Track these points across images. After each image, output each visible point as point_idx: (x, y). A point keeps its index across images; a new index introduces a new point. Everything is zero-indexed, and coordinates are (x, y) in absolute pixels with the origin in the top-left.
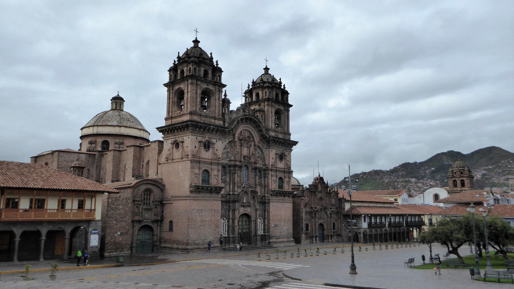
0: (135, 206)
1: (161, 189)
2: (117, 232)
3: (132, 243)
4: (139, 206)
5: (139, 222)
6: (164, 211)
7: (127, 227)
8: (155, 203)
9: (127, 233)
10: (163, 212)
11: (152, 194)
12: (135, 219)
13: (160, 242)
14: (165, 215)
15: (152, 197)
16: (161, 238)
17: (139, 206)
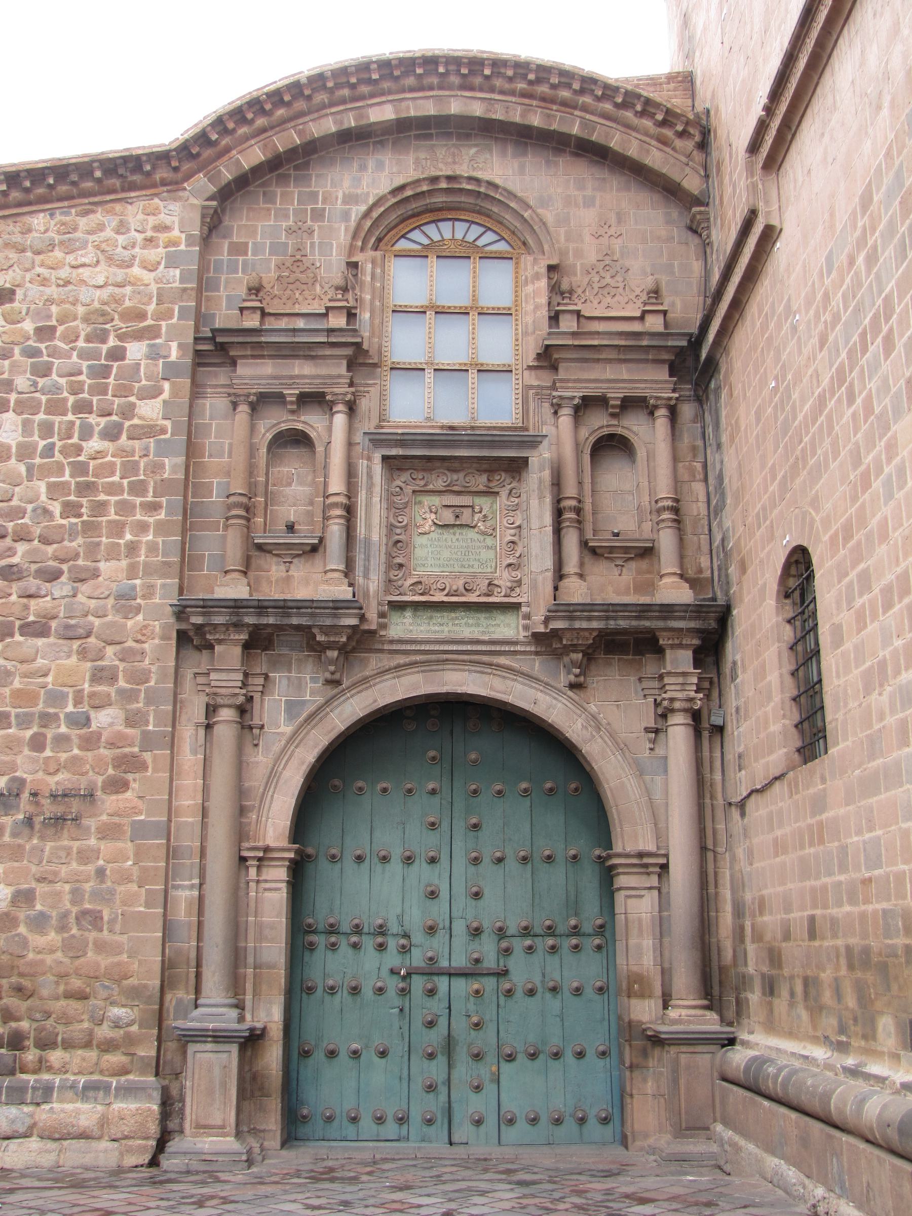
1: (669, 190)
3: (177, 972)
5: (341, 641)
8: (581, 379)
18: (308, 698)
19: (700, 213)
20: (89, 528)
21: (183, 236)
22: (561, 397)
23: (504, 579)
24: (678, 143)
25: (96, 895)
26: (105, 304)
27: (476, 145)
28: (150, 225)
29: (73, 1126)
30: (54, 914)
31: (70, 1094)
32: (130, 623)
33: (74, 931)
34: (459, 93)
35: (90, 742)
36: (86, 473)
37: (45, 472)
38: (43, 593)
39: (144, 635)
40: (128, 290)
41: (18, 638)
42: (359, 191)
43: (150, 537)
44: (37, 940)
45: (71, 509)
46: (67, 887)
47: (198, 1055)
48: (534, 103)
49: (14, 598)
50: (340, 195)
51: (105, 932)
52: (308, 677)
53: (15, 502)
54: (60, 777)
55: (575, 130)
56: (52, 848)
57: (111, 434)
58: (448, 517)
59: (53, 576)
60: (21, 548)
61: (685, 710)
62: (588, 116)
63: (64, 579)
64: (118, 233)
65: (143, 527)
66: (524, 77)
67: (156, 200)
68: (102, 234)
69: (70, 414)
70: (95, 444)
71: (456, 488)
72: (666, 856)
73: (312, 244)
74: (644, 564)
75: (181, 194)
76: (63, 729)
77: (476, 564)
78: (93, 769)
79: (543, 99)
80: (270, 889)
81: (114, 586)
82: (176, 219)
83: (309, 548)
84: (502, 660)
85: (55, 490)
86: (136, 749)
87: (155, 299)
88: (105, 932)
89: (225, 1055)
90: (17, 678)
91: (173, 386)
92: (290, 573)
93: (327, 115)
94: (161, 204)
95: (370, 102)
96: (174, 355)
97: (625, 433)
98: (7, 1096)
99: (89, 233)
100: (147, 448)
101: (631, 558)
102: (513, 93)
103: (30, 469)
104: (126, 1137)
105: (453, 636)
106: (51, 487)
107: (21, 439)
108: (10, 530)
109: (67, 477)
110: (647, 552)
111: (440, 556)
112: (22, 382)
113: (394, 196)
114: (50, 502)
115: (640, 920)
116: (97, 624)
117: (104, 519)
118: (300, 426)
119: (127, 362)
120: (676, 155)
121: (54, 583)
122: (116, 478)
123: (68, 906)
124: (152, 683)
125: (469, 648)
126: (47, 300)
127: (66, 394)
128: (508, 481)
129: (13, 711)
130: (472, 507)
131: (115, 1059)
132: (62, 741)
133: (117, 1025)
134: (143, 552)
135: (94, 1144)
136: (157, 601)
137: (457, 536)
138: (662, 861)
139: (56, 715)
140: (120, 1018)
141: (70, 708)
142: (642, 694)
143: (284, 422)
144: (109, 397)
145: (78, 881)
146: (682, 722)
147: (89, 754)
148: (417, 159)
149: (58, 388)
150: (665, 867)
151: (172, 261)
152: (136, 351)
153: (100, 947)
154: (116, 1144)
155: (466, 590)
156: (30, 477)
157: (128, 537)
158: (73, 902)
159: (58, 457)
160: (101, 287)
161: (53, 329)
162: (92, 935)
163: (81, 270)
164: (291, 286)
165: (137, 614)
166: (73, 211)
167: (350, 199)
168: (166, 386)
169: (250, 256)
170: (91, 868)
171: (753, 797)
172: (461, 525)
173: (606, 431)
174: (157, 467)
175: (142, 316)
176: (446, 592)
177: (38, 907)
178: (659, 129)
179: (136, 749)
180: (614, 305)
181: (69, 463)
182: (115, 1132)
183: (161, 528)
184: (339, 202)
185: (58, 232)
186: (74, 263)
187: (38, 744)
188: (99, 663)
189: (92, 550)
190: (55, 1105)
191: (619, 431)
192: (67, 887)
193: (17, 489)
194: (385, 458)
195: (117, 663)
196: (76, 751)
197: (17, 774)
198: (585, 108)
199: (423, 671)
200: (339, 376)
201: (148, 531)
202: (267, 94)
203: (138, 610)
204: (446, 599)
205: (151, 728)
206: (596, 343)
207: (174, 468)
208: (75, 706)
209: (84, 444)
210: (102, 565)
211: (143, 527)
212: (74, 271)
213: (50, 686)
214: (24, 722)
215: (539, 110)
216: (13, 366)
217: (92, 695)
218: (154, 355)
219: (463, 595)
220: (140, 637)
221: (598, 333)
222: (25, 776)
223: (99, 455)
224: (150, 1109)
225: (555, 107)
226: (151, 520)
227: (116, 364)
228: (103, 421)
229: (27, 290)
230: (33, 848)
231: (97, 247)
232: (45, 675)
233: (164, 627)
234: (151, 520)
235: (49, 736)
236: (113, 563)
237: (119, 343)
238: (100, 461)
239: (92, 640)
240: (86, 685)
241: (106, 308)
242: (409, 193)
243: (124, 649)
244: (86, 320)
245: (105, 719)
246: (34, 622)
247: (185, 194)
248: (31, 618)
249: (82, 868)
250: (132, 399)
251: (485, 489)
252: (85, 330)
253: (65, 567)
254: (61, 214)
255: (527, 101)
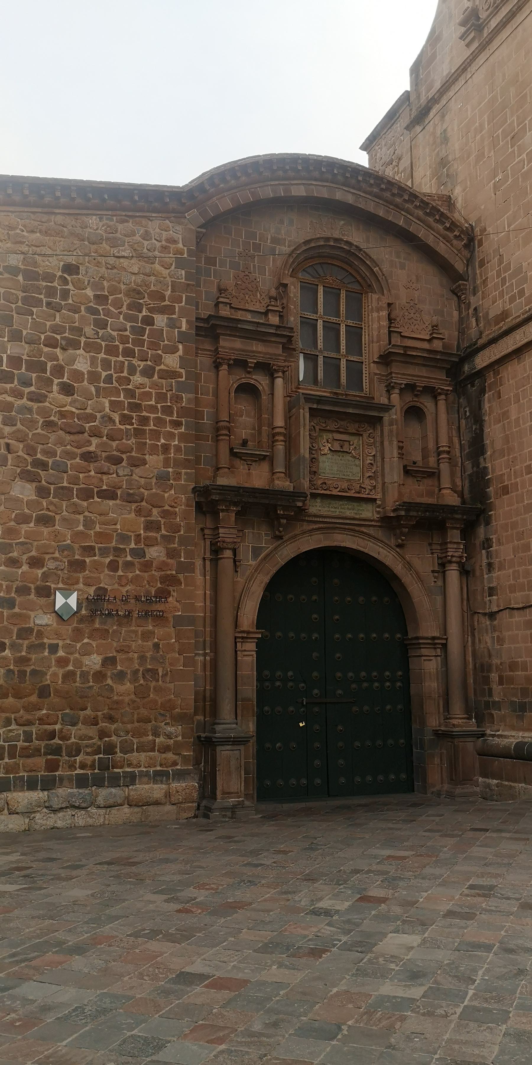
0: (230, 380)
2: (46, 593)
3: (209, 704)
4: (261, 381)
6: (493, 433)
7: (155, 553)
8: (403, 374)
9: (150, 608)
10: (477, 447)
11: (373, 300)
12: (222, 481)
13: (480, 711)
14: (496, 466)
15: (375, 324)
16: (483, 670)
17: (261, 381)
18: (264, 545)
19: (463, 284)
20: (138, 433)
21: (185, 249)
22: (395, 383)
23: (367, 484)
24: (455, 242)
25: (153, 658)
26: (139, 286)
27: (343, 220)
28: (164, 238)
29: (150, 798)
30: (129, 672)
31: (145, 779)
32: (166, 495)
33: (142, 682)
34: (341, 187)
35: (147, 566)
36: (133, 396)
37: (108, 393)
38: (111, 472)
39: (176, 503)
40: (153, 278)
41: (96, 499)
42: (280, 237)
43: (176, 443)
44: (121, 688)
45: (126, 419)
46: (136, 655)
47: (223, 752)
48: (381, 202)
49: (92, 473)
50: (269, 237)
51: (160, 682)
52: (263, 533)
53: (89, 411)
54: (128, 588)
55: (401, 223)
56: (125, 631)
57: (148, 372)
58: (337, 447)
59: (117, 461)
60: (95, 441)
61: (456, 562)
62: (408, 216)
63: (124, 464)
64: (144, 239)
65: (171, 436)
66: (378, 185)
67: (167, 221)
68: (134, 238)
69: (120, 356)
70: (138, 379)
71: (341, 430)
72: (447, 639)
73: (254, 266)
74: (429, 482)
75: (183, 220)
76: (129, 558)
77: (351, 474)
78: (149, 584)
79: (386, 201)
80: (247, 655)
81: (156, 471)
82: (180, 237)
83: (262, 457)
84: (357, 528)
85: (115, 405)
86: (174, 572)
87: (170, 288)
88: (160, 682)
89: (238, 752)
90: (98, 525)
91: (184, 347)
92: (250, 471)
93: (268, 186)
94: (170, 225)
95: (292, 182)
96: (184, 328)
97: (421, 406)
98: (108, 782)
99: (126, 236)
100: (171, 386)
101: (424, 477)
102: (370, 193)
103: (98, 389)
104: (182, 803)
105: (342, 515)
106: (111, 403)
107: (89, 369)
108: (87, 429)
109: (122, 398)
110: (434, 475)
111: (336, 468)
112: (89, 330)
113: (305, 246)
114: (112, 413)
115: (430, 673)
116: (146, 494)
117: (147, 428)
118: (252, 382)
119: (155, 327)
120: (452, 248)
121: (118, 466)
122: (153, 403)
123: (137, 667)
124: (182, 533)
125: (348, 521)
126: (101, 277)
127: (117, 343)
128: (369, 428)
129: (97, 546)
130: (349, 442)
131: (170, 756)
132: (129, 565)
133: (169, 736)
134: (172, 451)
135: (160, 808)
136: (183, 482)
137: (341, 457)
138: (444, 642)
139: (125, 549)
140: (171, 733)
141: (133, 546)
142: (430, 552)
143: (243, 378)
144: (145, 349)
145: (143, 652)
146: (455, 568)
147: (146, 575)
148: (311, 222)
149: (113, 338)
150: (445, 646)
151: (180, 264)
152: (160, 320)
153: (158, 690)
154: (175, 807)
155: (349, 489)
156: (98, 396)
157: (163, 441)
158: (140, 665)
159: (115, 384)
160: (136, 274)
161: (106, 298)
162: (153, 684)
163: (122, 260)
164: (243, 291)
165: (171, 490)
166: (115, 218)
167: (275, 241)
168: (180, 347)
169: (217, 267)
170: (150, 644)
171: (507, 610)
172: (344, 452)
173: (412, 404)
174: (178, 399)
175: (163, 298)
176: (338, 489)
177: (119, 668)
178: (445, 232)
179: (174, 572)
180: (417, 330)
181: (123, 389)
182: (173, 799)
183: (183, 437)
184: (269, 241)
185: (106, 231)
186: (117, 254)
187: (113, 566)
188: (149, 518)
189: (141, 446)
190: (138, 786)
191: (418, 404)
192: (136, 655)
193: (90, 402)
194: (310, 409)
195: (160, 519)
196: (138, 572)
197: (101, 585)
198: (408, 211)
199: (322, 533)
200: (280, 355)
201: (175, 438)
202: (239, 166)
203: (171, 486)
204: (340, 494)
205: (182, 560)
206: (414, 354)
207: (189, 400)
208: (136, 545)
209: (131, 377)
210: (147, 457)
211: (171, 436)
212: (117, 260)
213: (119, 531)
214: (104, 552)
215: (383, 206)
216: (82, 317)
217: (146, 538)
218: (172, 324)
219: (347, 492)
220: (173, 504)
221: (417, 348)
222: (106, 587)
223: (141, 387)
224: (193, 785)
225: (391, 207)
226: (176, 432)
227: (148, 328)
228: (142, 364)
229: (87, 267)
230: (114, 631)
231: (132, 246)
232: (115, 524)
233: (188, 499)
234: (176, 432)
235: (120, 563)
236: (155, 457)
237: (149, 314)
238: (142, 390)
239: (144, 503)
240: (142, 532)
241: (139, 288)
242: (313, 245)
243: (164, 510)
244: (127, 295)
245: (155, 553)
246: (105, 490)
247: (186, 221)
248: (105, 487)
249: (145, 643)
250: (160, 352)
251: (356, 432)
252: (127, 301)
253: (124, 456)
254: (107, 219)
255: (377, 200)
